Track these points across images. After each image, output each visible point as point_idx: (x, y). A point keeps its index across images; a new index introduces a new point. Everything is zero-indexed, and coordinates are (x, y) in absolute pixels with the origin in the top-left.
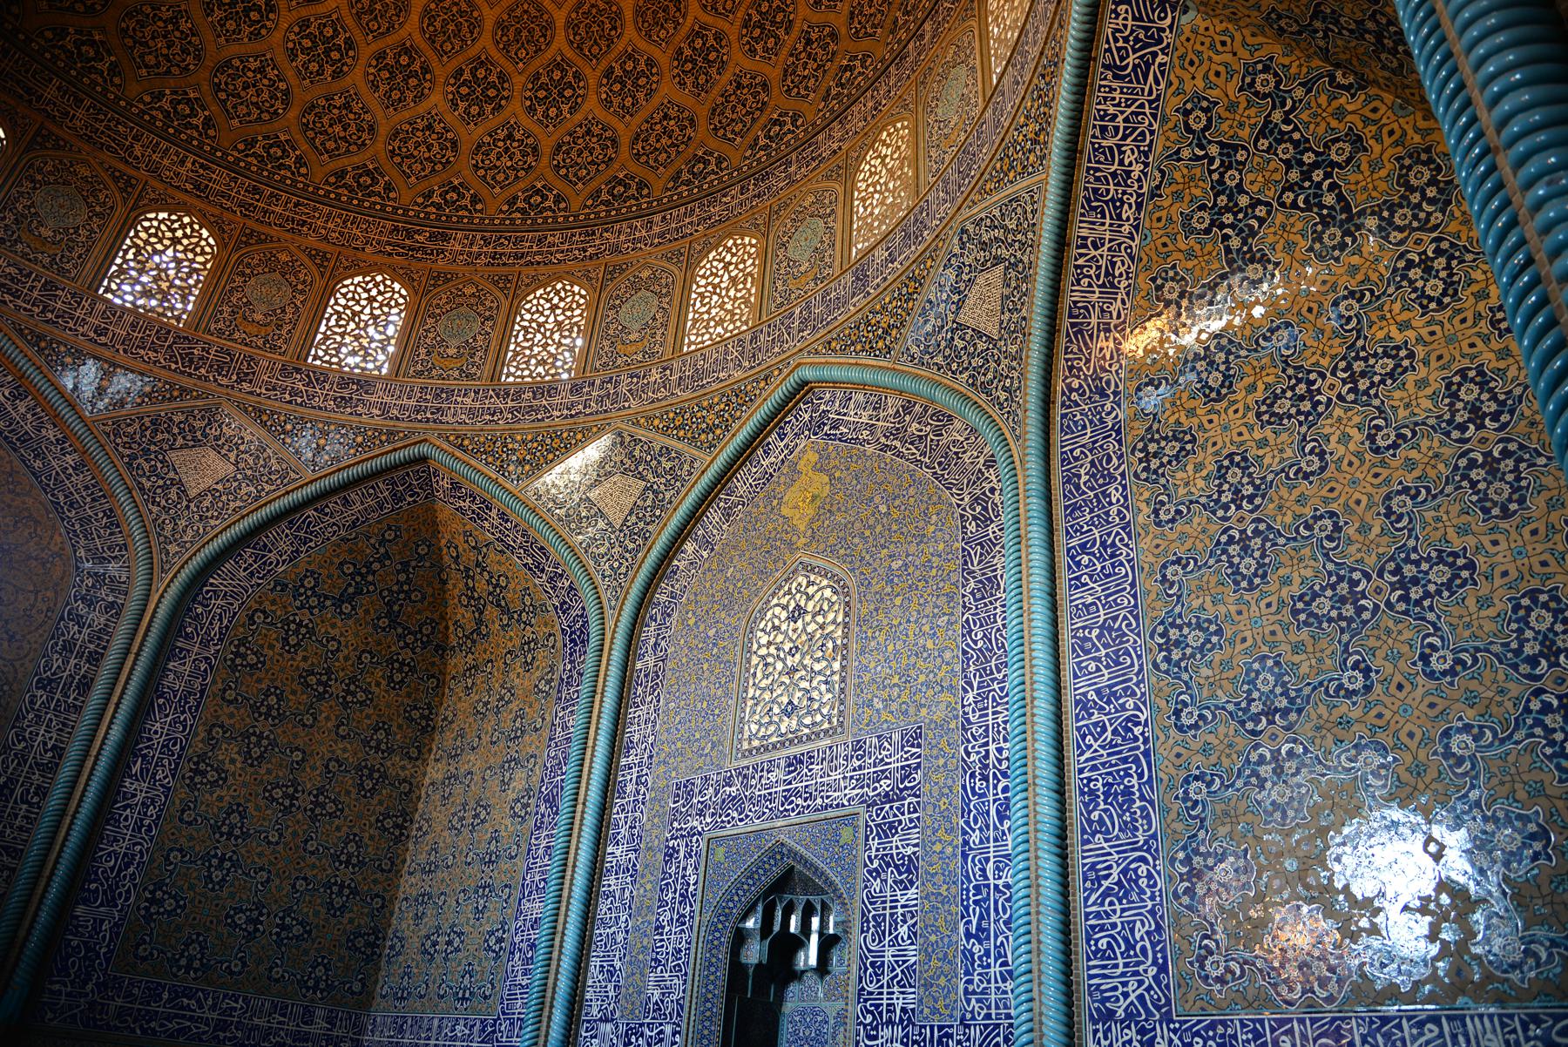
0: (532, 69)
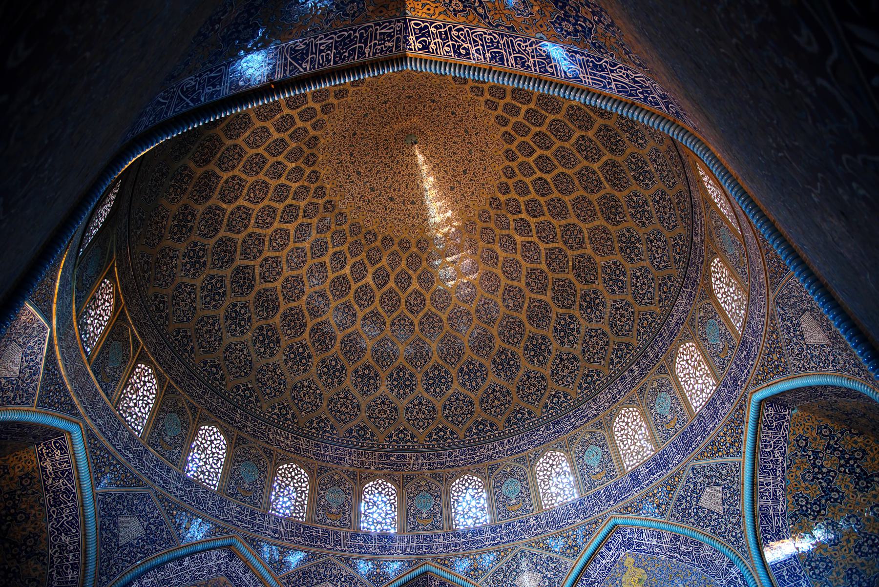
0: (424, 370)
